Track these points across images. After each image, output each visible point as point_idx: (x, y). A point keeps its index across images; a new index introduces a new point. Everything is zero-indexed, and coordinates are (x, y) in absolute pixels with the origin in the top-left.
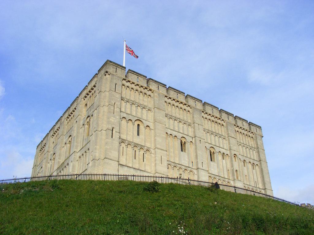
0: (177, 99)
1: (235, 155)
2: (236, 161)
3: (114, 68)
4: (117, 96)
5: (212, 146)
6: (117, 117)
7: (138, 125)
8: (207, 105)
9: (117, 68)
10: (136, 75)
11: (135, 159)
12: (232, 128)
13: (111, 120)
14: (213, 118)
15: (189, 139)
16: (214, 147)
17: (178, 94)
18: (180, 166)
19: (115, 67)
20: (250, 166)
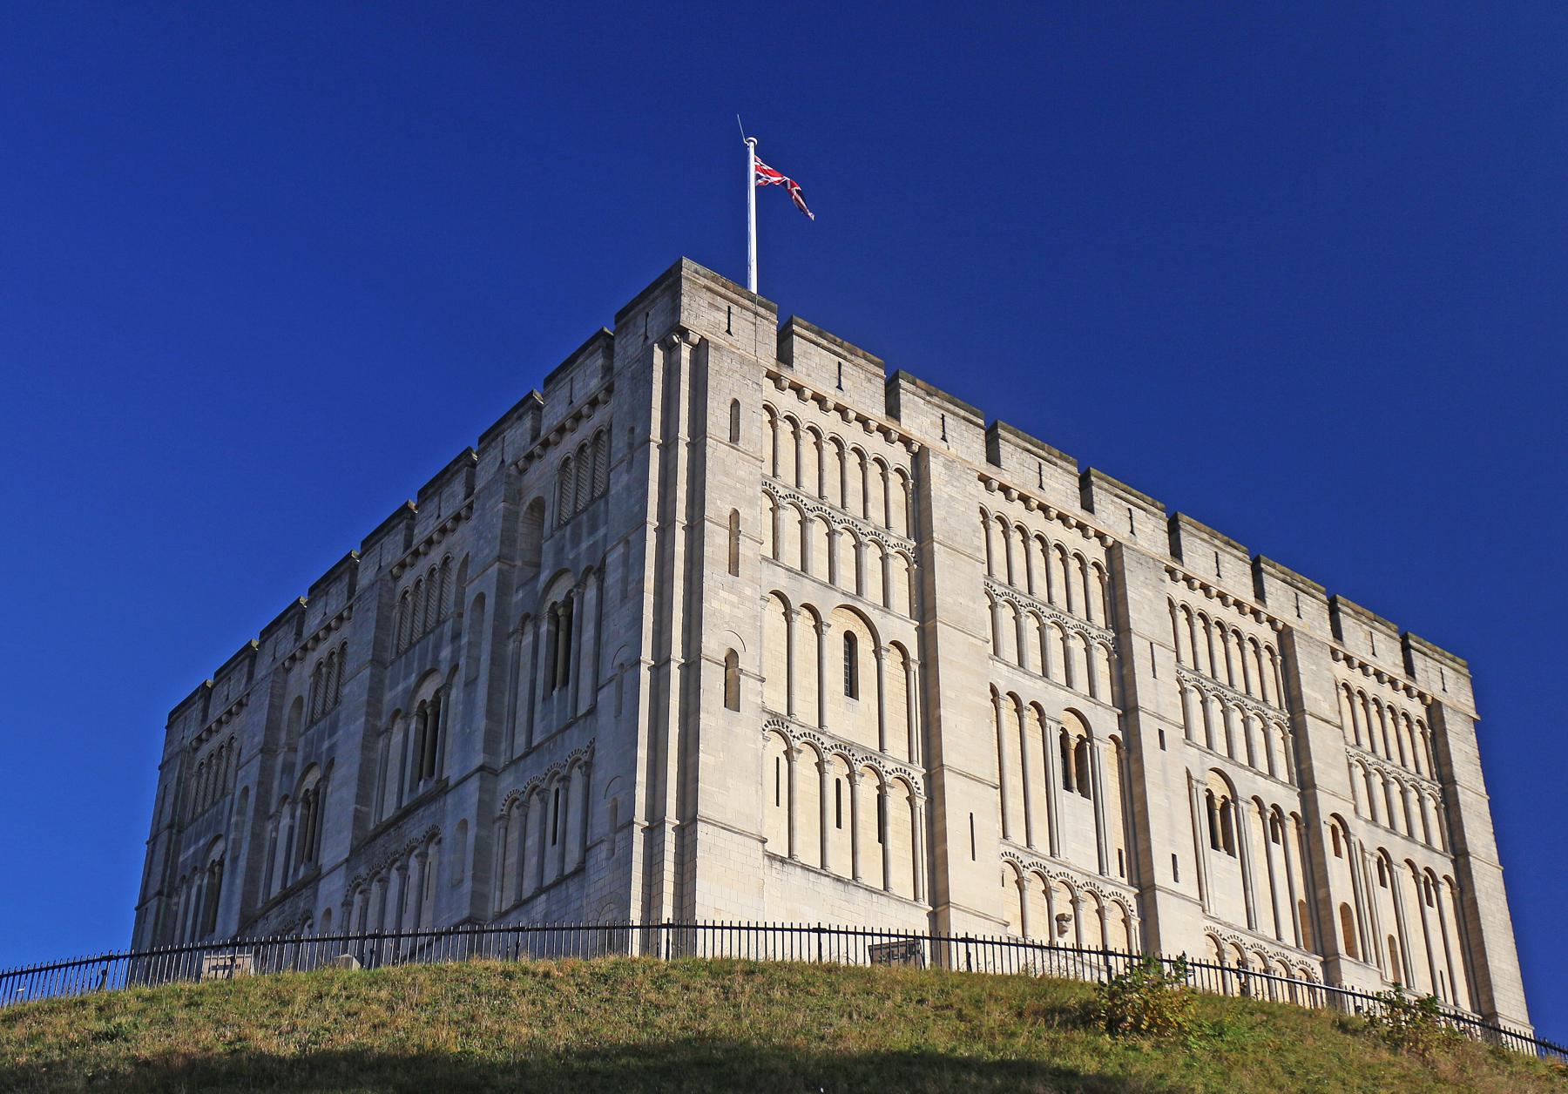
0: (1037, 497)
2: (1338, 853)
3: (718, 309)
4: (741, 473)
5: (1218, 764)
6: (748, 591)
7: (850, 638)
8: (1187, 531)
9: (734, 309)
10: (829, 350)
11: (839, 825)
12: (1318, 665)
13: (715, 604)
16: (1229, 769)
17: (1046, 467)
19: (724, 304)
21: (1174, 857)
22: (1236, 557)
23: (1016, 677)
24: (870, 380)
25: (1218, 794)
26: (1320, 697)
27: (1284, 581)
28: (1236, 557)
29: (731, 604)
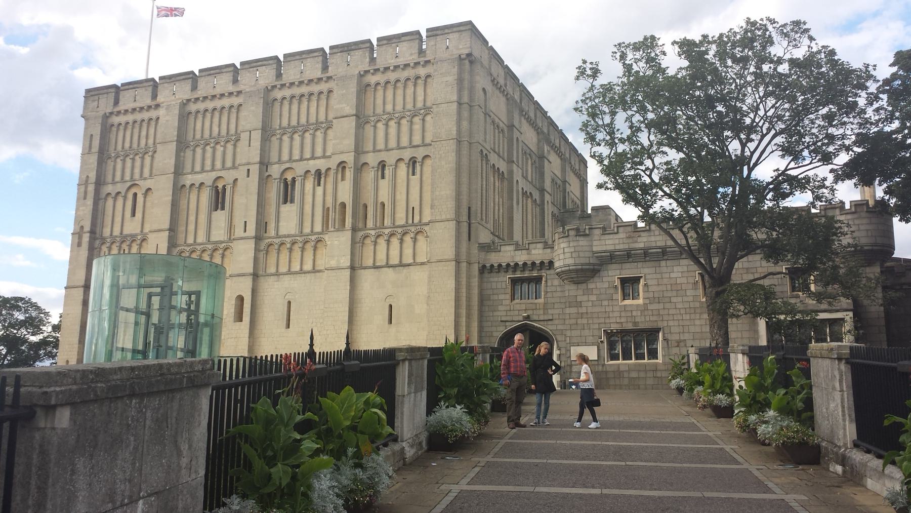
1: (343, 165)
2: (343, 179)
5: (288, 165)
14: (304, 89)
15: (229, 176)
18: (202, 246)
20: (403, 170)
21: (246, 222)
22: (313, 57)
23: (195, 177)
24: (146, 90)
25: (289, 179)
26: (344, 105)
27: (341, 52)
28: (313, 57)
29: (83, 211)
